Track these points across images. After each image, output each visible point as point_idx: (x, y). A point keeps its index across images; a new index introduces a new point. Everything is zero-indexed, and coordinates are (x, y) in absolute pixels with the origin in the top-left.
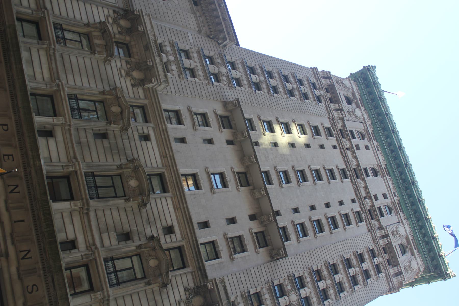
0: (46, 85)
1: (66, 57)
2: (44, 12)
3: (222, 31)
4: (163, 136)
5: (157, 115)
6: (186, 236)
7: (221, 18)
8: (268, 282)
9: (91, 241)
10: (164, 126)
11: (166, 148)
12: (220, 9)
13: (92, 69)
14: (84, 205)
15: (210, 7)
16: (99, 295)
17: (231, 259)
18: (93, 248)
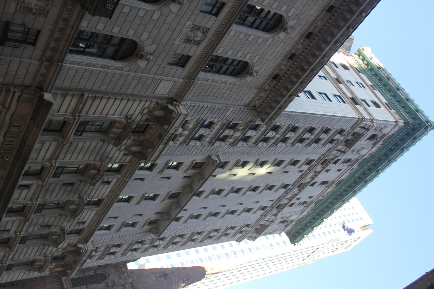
0: (42, 164)
1: (75, 144)
2: (75, 119)
3: (268, 114)
4: (121, 184)
5: (129, 172)
6: (91, 226)
7: (279, 106)
8: (134, 241)
9: (19, 230)
10: (127, 179)
11: (117, 190)
12: (288, 98)
13: (94, 147)
14: (25, 220)
15: (282, 90)
16: (8, 249)
17: (117, 231)
18: (18, 233)
